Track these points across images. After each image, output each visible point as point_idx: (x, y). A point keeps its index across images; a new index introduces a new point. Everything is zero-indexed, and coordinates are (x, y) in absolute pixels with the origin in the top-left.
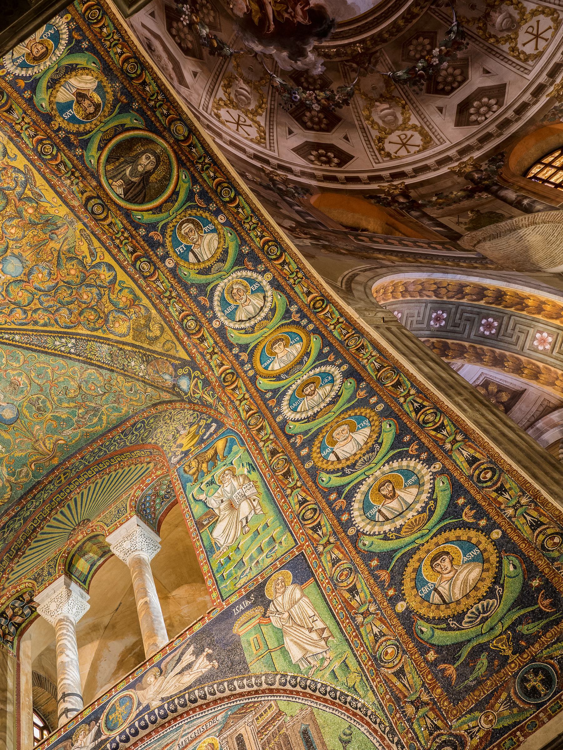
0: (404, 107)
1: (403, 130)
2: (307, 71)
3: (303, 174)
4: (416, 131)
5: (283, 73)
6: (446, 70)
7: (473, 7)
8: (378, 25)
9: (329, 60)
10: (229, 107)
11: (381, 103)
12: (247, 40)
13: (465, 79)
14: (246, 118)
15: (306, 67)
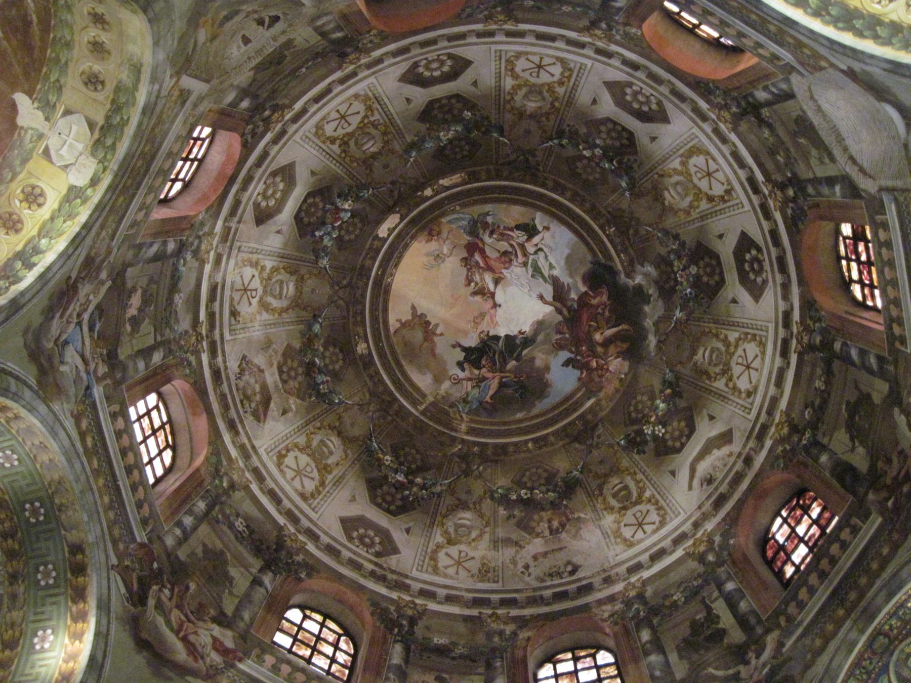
0: (662, 176)
1: (691, 176)
2: (656, 282)
3: (786, 296)
4: (687, 162)
5: (669, 309)
6: (604, 140)
7: (528, 132)
8: (579, 216)
9: (635, 260)
10: (732, 375)
11: (664, 199)
12: (649, 353)
13: (609, 120)
14: (737, 354)
15: (652, 283)
